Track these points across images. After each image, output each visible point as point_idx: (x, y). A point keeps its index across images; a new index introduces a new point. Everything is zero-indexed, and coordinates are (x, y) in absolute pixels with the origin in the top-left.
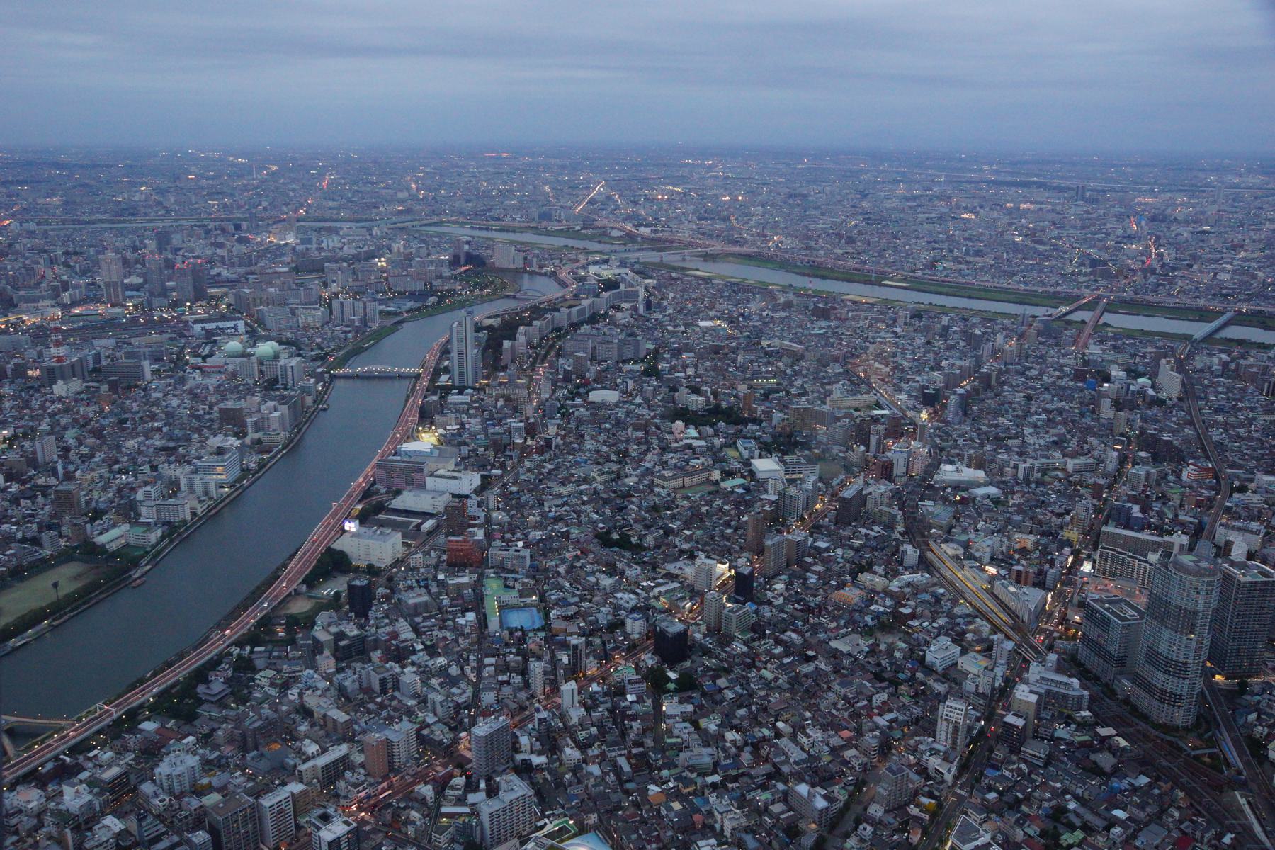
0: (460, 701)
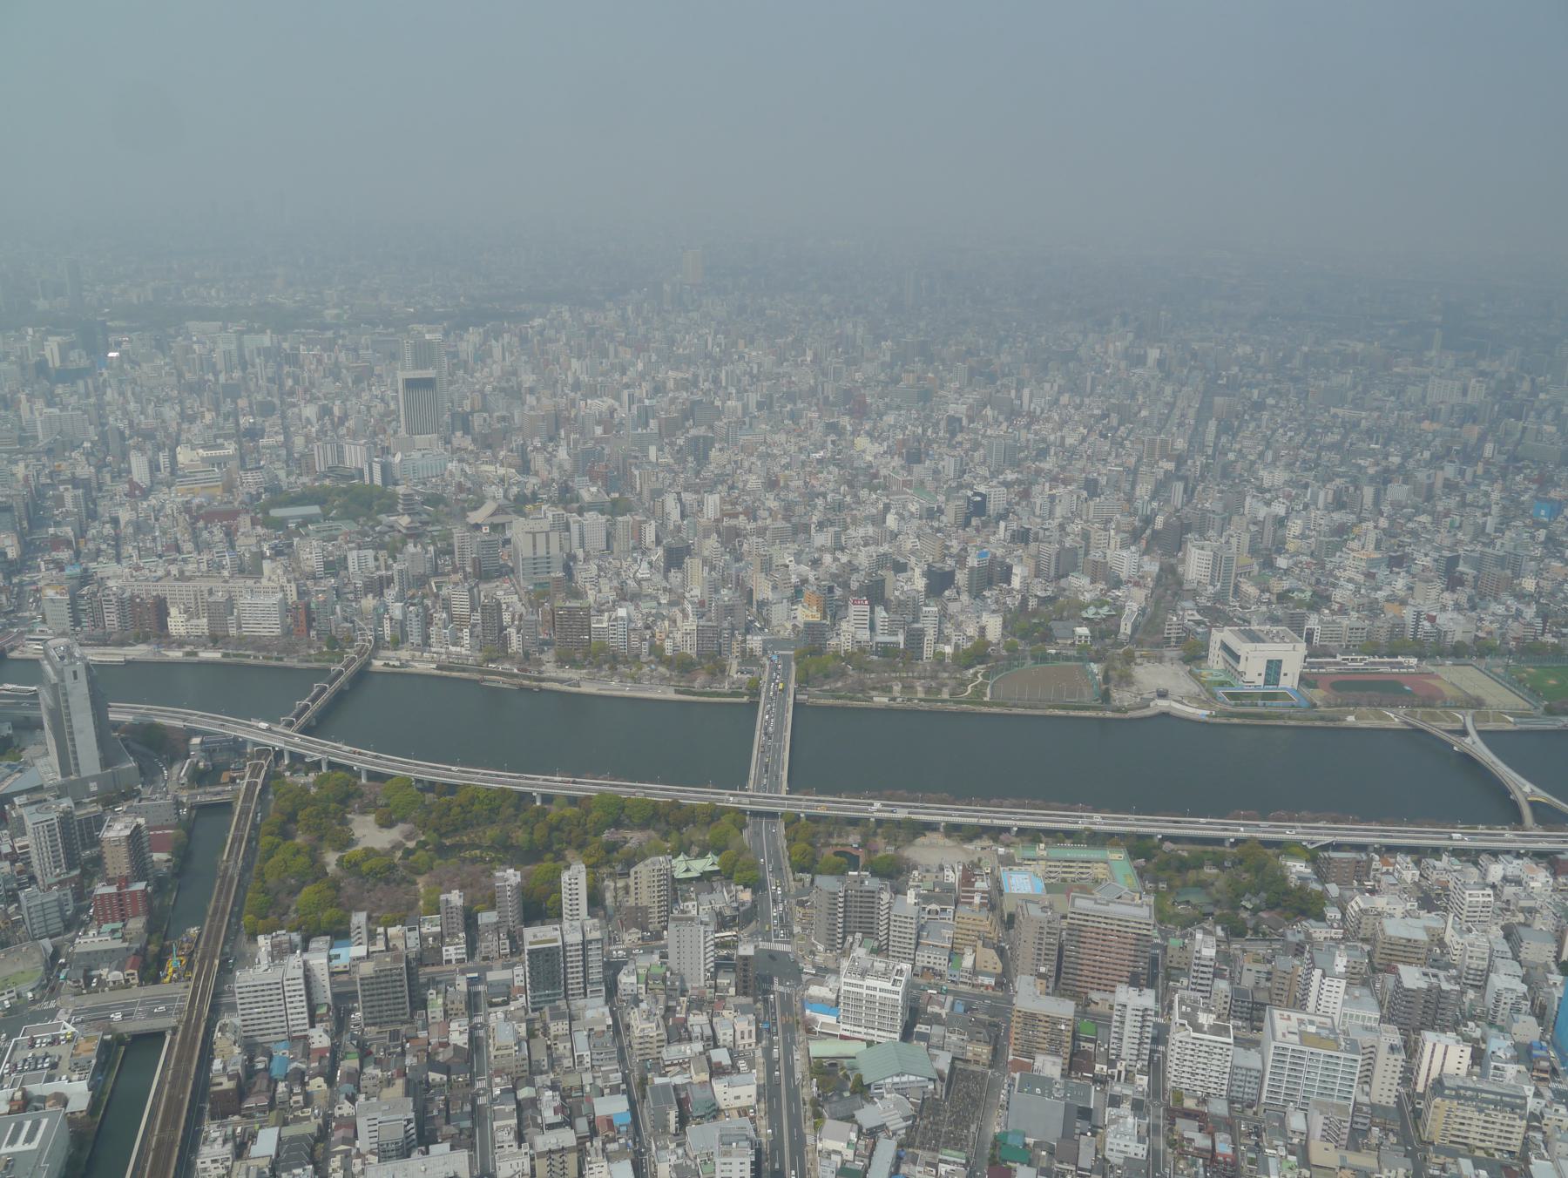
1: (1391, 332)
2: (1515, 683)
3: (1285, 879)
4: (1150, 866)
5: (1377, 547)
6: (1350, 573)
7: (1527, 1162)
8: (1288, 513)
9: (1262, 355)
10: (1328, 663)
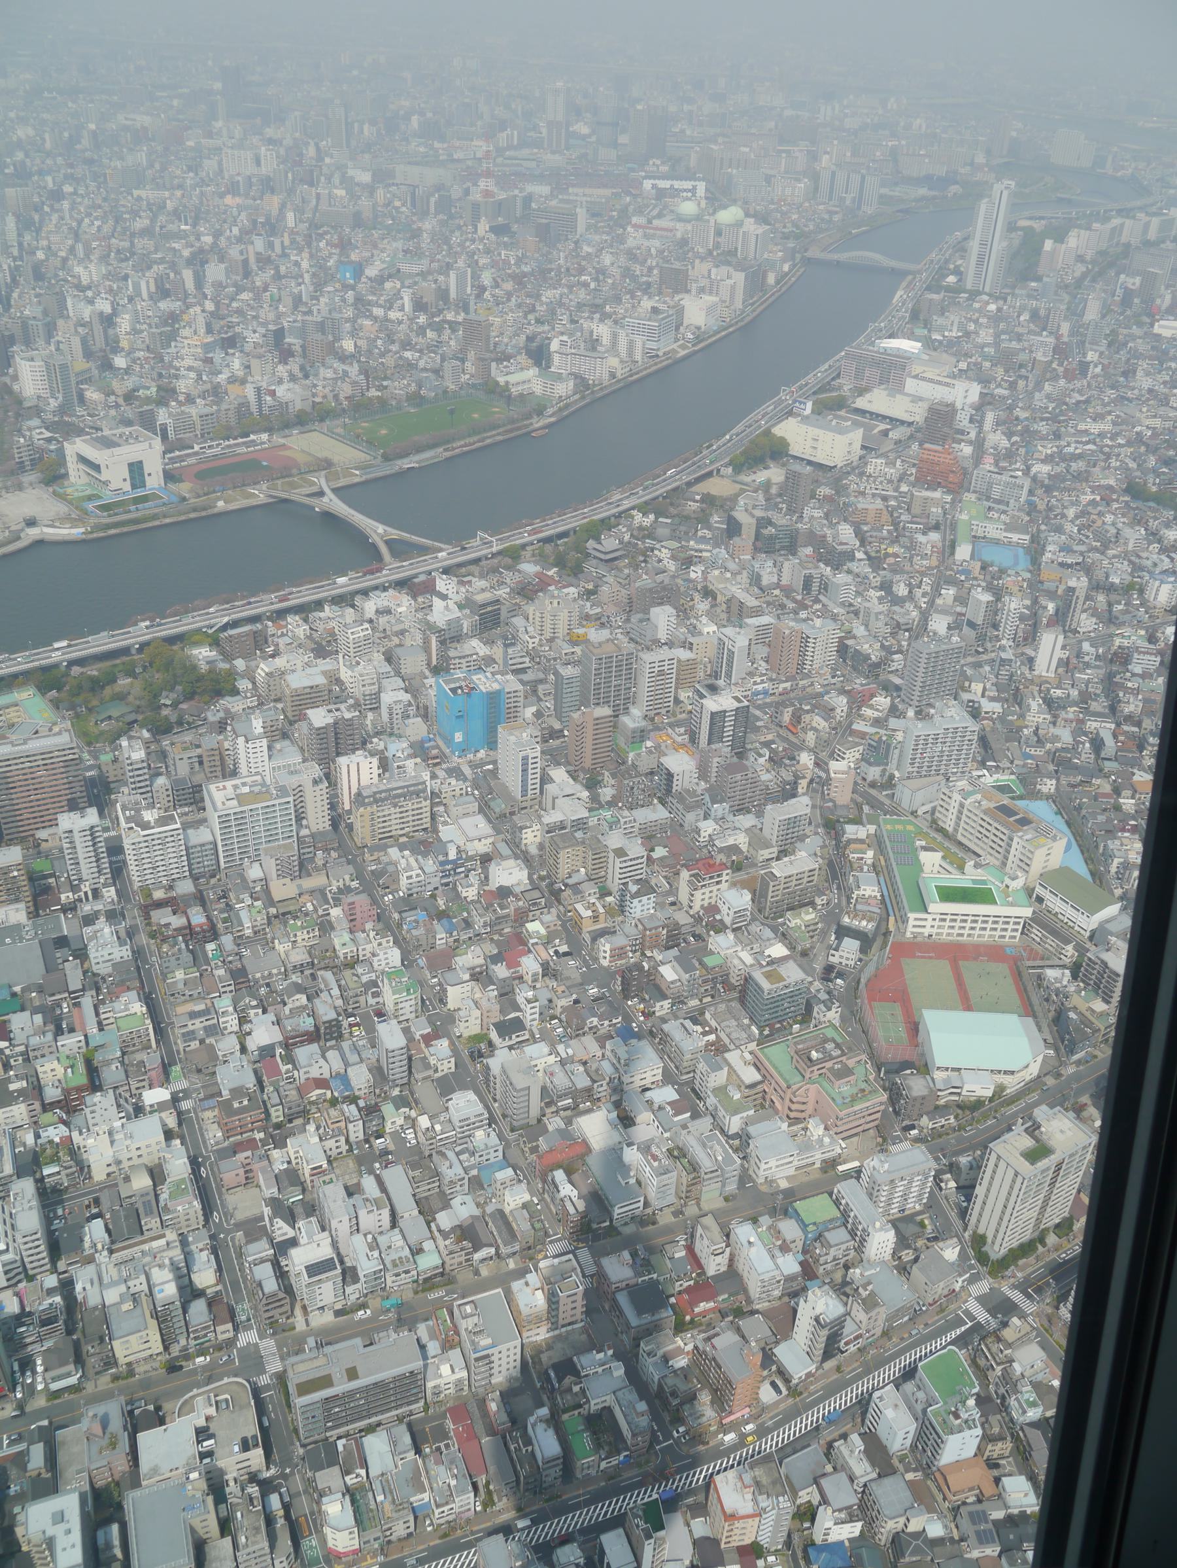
0: (901, 621)
1: (175, 102)
2: (355, 439)
3: (194, 667)
4: (63, 695)
5: (209, 330)
6: (188, 362)
7: (436, 831)
8: (114, 309)
9: (47, 136)
10: (188, 455)
